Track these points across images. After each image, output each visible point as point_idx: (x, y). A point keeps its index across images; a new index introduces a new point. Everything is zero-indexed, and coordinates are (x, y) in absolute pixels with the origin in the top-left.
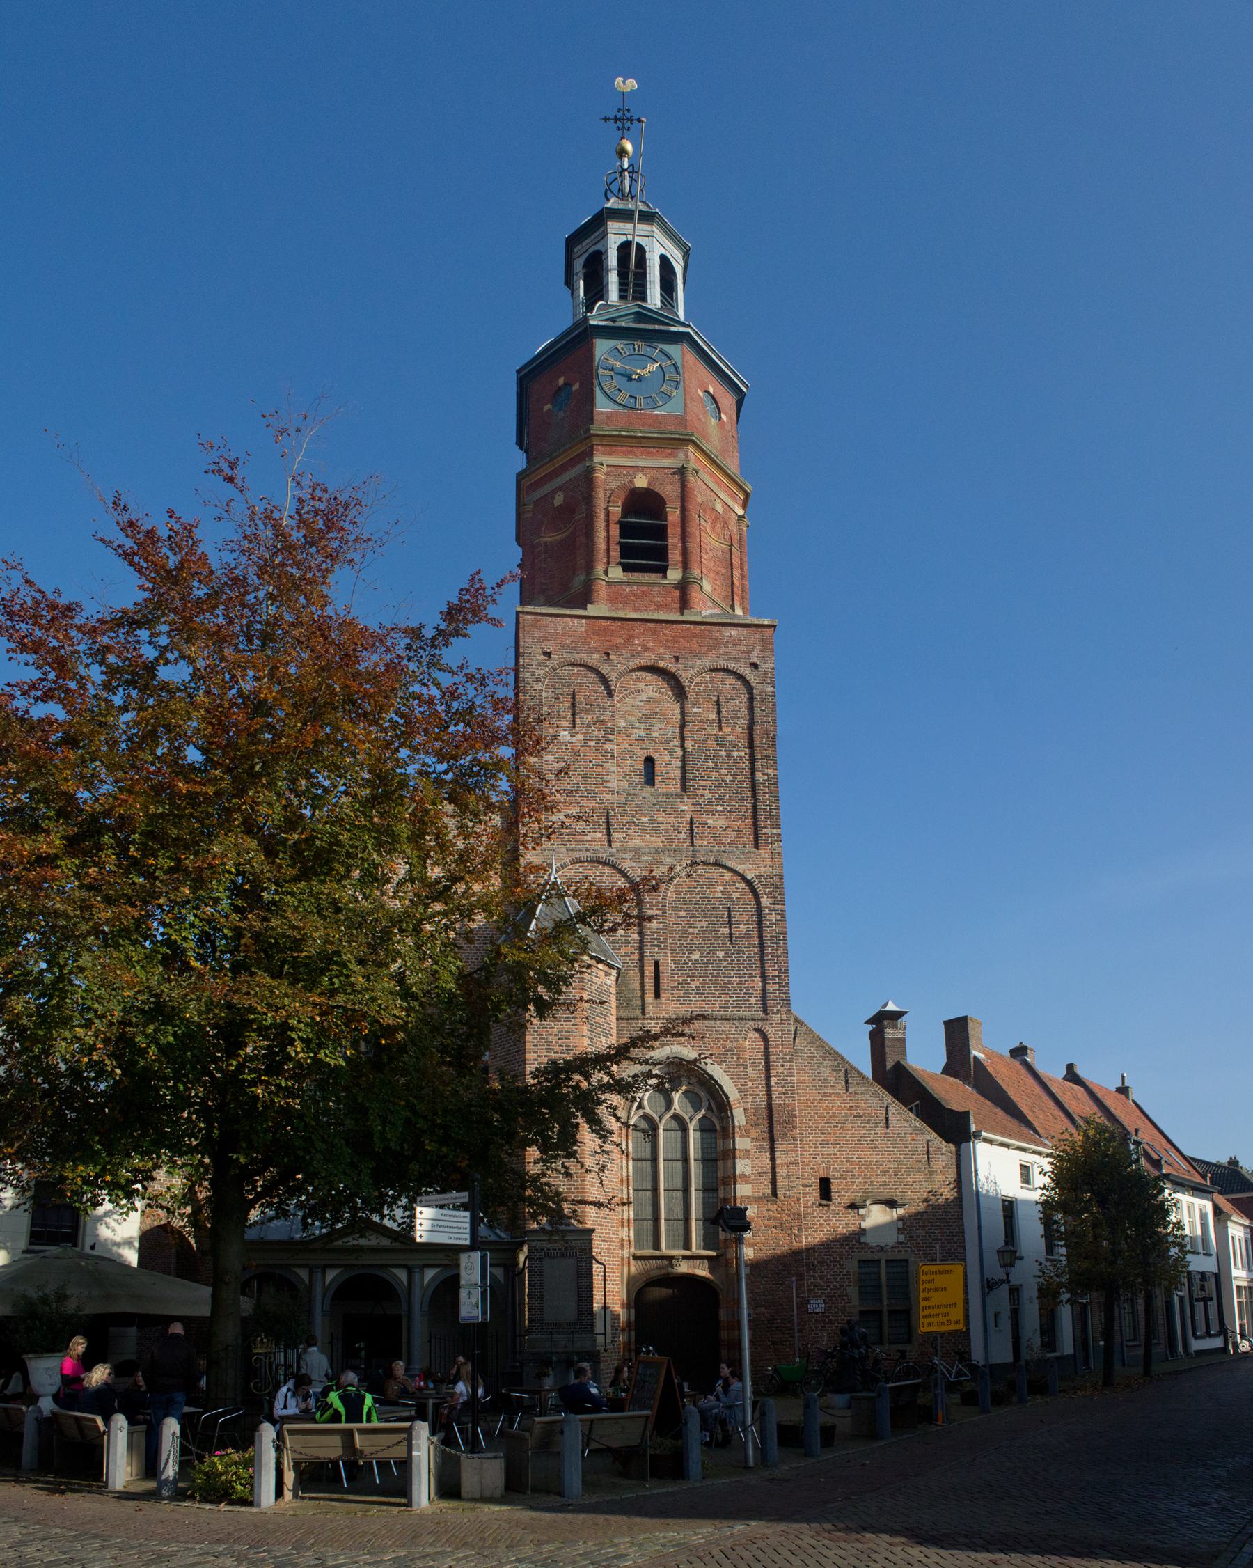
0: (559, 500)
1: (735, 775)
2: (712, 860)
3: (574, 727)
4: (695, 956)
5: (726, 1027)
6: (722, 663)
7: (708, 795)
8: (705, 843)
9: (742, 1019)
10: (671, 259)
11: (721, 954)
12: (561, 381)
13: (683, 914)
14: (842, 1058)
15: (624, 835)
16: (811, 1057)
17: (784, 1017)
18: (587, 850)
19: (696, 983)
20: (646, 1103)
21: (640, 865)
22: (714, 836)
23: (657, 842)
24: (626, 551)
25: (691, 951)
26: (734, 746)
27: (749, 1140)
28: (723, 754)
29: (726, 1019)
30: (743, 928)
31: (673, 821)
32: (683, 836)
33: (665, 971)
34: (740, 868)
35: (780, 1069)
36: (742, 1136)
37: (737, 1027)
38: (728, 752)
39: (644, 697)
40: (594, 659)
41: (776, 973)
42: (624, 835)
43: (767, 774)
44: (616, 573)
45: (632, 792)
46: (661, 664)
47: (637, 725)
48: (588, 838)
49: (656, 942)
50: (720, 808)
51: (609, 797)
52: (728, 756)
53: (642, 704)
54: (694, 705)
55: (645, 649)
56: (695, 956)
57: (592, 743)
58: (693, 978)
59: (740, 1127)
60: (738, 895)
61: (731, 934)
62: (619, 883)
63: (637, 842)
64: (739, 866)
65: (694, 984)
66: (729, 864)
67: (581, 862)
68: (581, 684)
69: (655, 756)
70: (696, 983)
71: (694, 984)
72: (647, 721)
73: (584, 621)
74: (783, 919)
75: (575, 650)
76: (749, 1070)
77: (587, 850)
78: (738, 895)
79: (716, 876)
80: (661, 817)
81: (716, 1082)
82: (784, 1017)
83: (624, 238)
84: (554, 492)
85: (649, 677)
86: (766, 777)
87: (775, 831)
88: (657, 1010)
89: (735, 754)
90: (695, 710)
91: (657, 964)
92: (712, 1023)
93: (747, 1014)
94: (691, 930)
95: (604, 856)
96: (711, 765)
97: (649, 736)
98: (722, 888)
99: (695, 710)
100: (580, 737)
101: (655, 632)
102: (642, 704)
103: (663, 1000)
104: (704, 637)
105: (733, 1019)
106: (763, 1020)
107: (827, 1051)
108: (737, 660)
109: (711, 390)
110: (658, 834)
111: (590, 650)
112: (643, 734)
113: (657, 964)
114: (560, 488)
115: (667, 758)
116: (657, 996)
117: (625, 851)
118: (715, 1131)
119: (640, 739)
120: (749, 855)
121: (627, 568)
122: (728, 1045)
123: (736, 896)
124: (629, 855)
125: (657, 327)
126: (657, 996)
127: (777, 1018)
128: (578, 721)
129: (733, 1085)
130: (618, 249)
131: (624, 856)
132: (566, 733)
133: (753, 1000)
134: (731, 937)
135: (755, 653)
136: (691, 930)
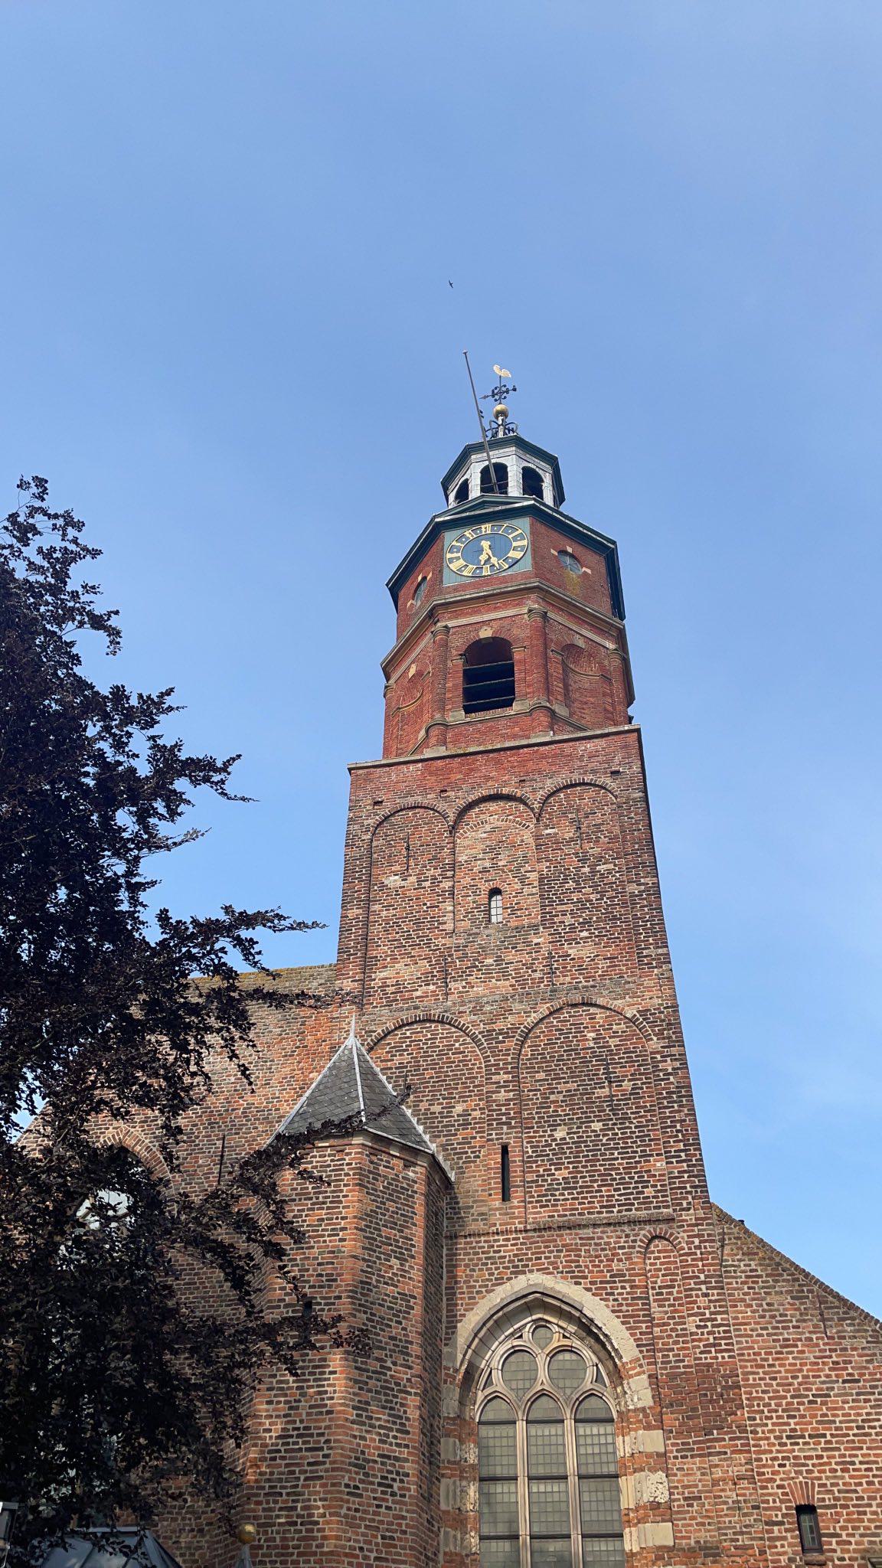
0: (412, 672)
1: (602, 893)
2: (578, 999)
3: (407, 869)
4: (560, 1134)
5: (610, 1237)
6: (576, 777)
7: (568, 920)
8: (568, 979)
9: (634, 1222)
10: (537, 470)
11: (597, 1126)
12: (420, 578)
13: (542, 1075)
14: (807, 1275)
15: (464, 983)
16: (752, 1276)
17: (701, 1213)
18: (416, 1008)
19: (565, 1173)
20: (497, 1376)
21: (482, 1017)
22: (580, 969)
23: (504, 986)
24: (468, 695)
25: (554, 1126)
26: (600, 859)
27: (658, 1434)
28: (587, 870)
29: (609, 1224)
30: (627, 1085)
31: (526, 958)
32: (537, 975)
33: (515, 1157)
34: (618, 1003)
35: (702, 1301)
36: (648, 1427)
37: (627, 1236)
38: (593, 867)
39: (488, 828)
40: (430, 799)
41: (681, 1146)
42: (464, 983)
43: (643, 884)
44: (457, 716)
45: (475, 930)
46: (505, 791)
47: (481, 856)
48: (419, 993)
50: (585, 934)
51: (447, 941)
52: (593, 872)
53: (485, 835)
54: (546, 826)
55: (488, 778)
56: (560, 1134)
57: (427, 884)
58: (559, 1166)
59: (643, 1409)
60: (617, 1041)
62: (457, 1045)
63: (479, 990)
64: (615, 1002)
65: (560, 1175)
66: (600, 1001)
67: (408, 1024)
68: (416, 827)
69: (503, 887)
70: (565, 1173)
71: (560, 1175)
72: (493, 851)
73: (420, 765)
74: (685, 1066)
75: (409, 794)
76: (655, 1308)
77: (416, 1008)
78: (617, 1041)
79: (586, 1021)
80: (511, 956)
81: (600, 1329)
82: (701, 1213)
83: (487, 463)
84: (409, 668)
85: (493, 806)
86: (643, 888)
87: (660, 951)
88: (506, 1218)
89: (602, 868)
90: (549, 831)
91: (505, 1150)
92: (589, 1232)
93: (643, 1214)
94: (553, 1097)
95: (436, 1012)
96: (571, 884)
97: (495, 866)
98: (593, 1035)
99: (549, 831)
100: (413, 879)
101: (498, 762)
102: (485, 835)
103: (515, 1202)
104: (555, 756)
105: (619, 1224)
106: (670, 1220)
107: (778, 1264)
108: (594, 772)
109: (570, 550)
110: (505, 975)
111: (425, 792)
112: (488, 864)
113: (505, 1150)
114: (413, 662)
115: (518, 886)
116: (506, 1197)
117: (463, 1004)
118: (611, 1420)
119: (485, 871)
120: (627, 986)
121: (468, 710)
122: (615, 1266)
123: (613, 1042)
124: (467, 1008)
125: (504, 507)
126: (506, 1197)
127: (689, 1217)
128: (412, 863)
129: (627, 1334)
130: (481, 472)
131: (461, 1009)
132: (397, 877)
133: (649, 1192)
135: (616, 760)
136: (553, 1097)
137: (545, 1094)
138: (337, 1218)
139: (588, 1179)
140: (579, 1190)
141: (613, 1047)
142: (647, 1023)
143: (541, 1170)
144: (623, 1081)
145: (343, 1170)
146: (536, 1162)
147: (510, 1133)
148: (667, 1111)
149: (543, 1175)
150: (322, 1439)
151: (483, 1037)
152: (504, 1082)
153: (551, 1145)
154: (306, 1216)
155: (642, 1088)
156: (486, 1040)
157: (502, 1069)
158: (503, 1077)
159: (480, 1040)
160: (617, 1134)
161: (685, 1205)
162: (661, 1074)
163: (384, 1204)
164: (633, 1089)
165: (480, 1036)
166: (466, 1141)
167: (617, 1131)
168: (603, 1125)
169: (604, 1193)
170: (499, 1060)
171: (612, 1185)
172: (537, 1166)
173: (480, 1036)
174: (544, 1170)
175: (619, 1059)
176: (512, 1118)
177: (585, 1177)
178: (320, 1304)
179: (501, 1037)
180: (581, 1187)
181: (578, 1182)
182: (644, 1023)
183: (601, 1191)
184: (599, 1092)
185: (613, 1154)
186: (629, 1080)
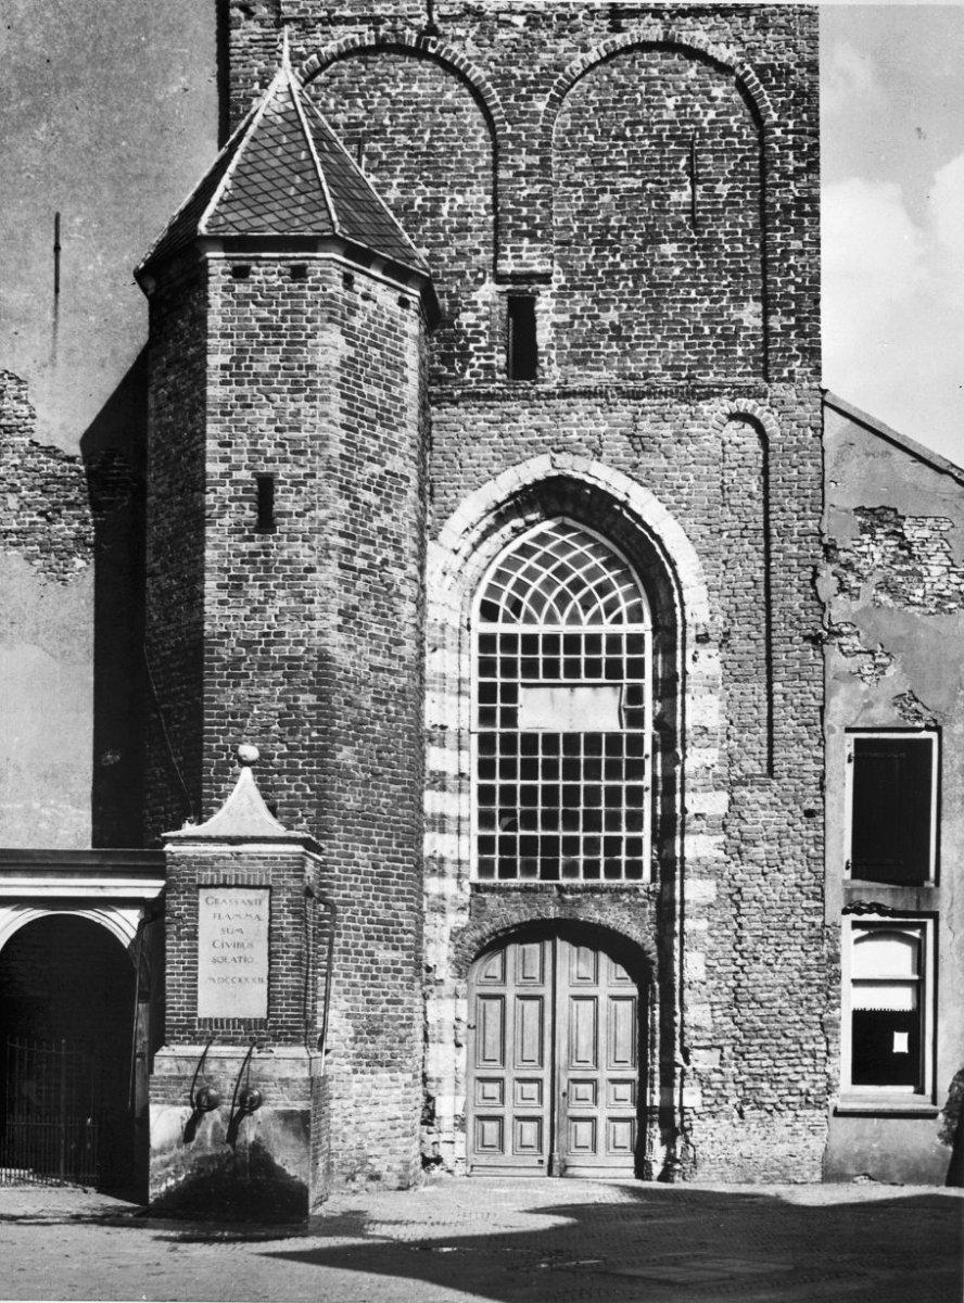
30: (723, 189)
49: (525, 227)
61: (693, 203)
78: (712, 114)
134: (692, 212)
137: (591, 191)
138: (300, 368)
139: (648, 327)
140: (634, 341)
141: (705, 125)
142: (766, 88)
143: (578, 308)
144: (717, 181)
145: (304, 296)
146: (571, 295)
147: (534, 249)
148: (779, 235)
149: (582, 317)
150: (302, 649)
151: (495, 86)
152: (528, 166)
153: (595, 272)
154: (251, 359)
155: (743, 196)
156: (499, 93)
157: (522, 144)
158: (523, 160)
159: (489, 91)
160: (697, 263)
161: (785, 374)
162: (777, 175)
163: (365, 349)
164: (729, 195)
165: (489, 85)
166: (461, 255)
167: (698, 258)
168: (679, 248)
169: (670, 349)
170: (521, 128)
171: (683, 338)
172: (571, 303)
173: (489, 85)
174: (583, 309)
175: (713, 144)
176: (537, 227)
177: (644, 324)
178: (284, 483)
179: (524, 91)
180: (637, 337)
181: (633, 329)
182: (761, 88)
183: (666, 346)
184: (675, 196)
185: (689, 293)
186: (726, 181)
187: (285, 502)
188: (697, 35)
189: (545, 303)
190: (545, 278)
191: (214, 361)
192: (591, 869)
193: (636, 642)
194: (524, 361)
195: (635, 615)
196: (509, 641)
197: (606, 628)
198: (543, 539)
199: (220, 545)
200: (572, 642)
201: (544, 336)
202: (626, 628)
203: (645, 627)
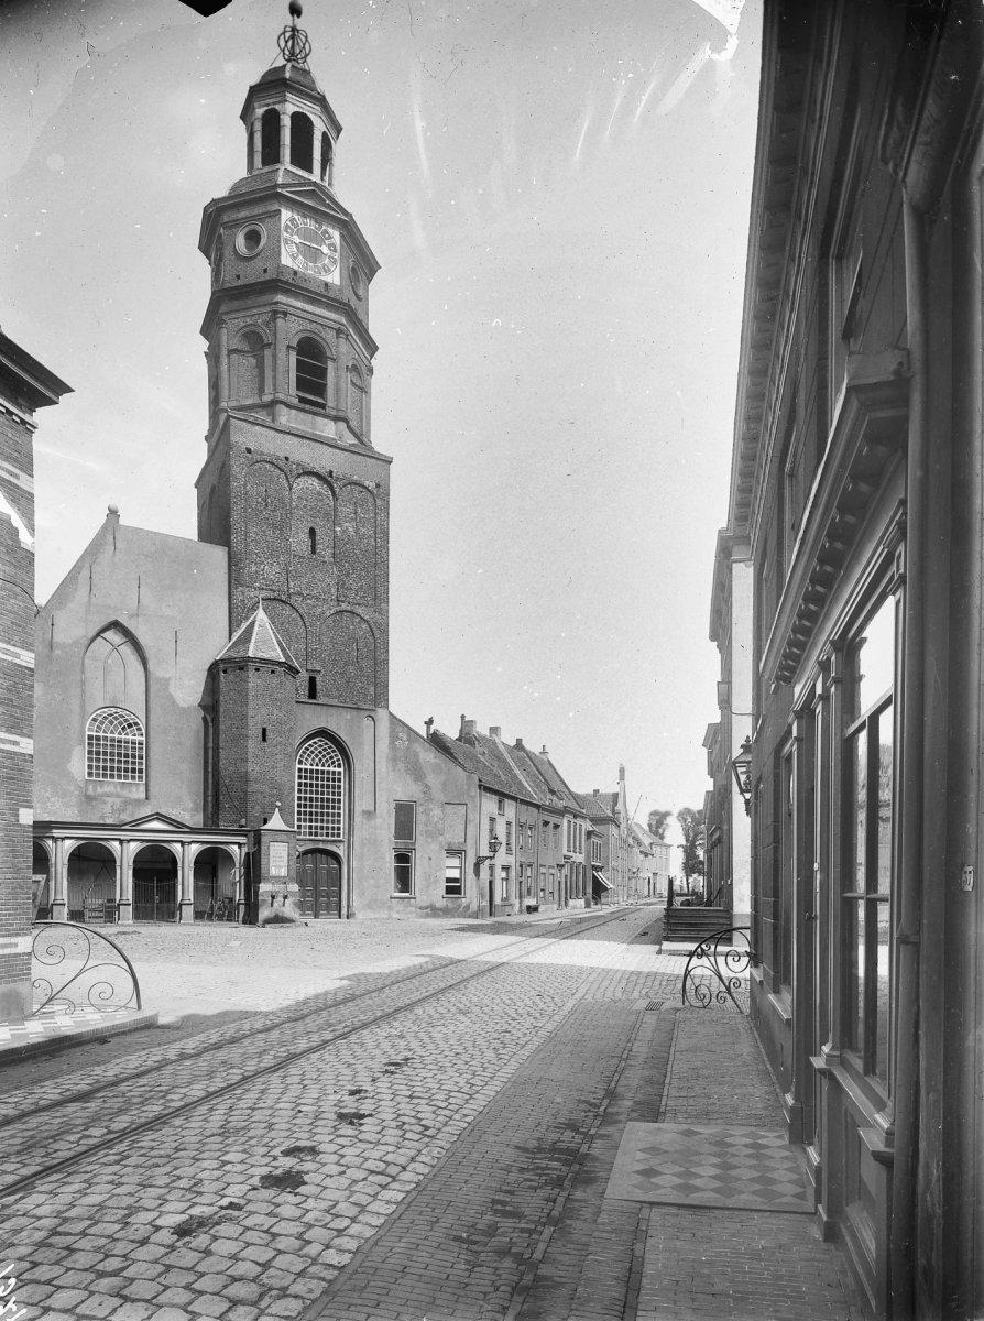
187: (269, 735)
188: (359, 610)
189: (319, 679)
190: (319, 672)
191: (251, 693)
192: (327, 835)
193: (339, 773)
194: (313, 694)
195: (339, 766)
196: (306, 770)
197: (332, 769)
198: (315, 743)
199: (253, 745)
200: (323, 772)
201: (319, 687)
202: (337, 769)
203: (342, 770)
